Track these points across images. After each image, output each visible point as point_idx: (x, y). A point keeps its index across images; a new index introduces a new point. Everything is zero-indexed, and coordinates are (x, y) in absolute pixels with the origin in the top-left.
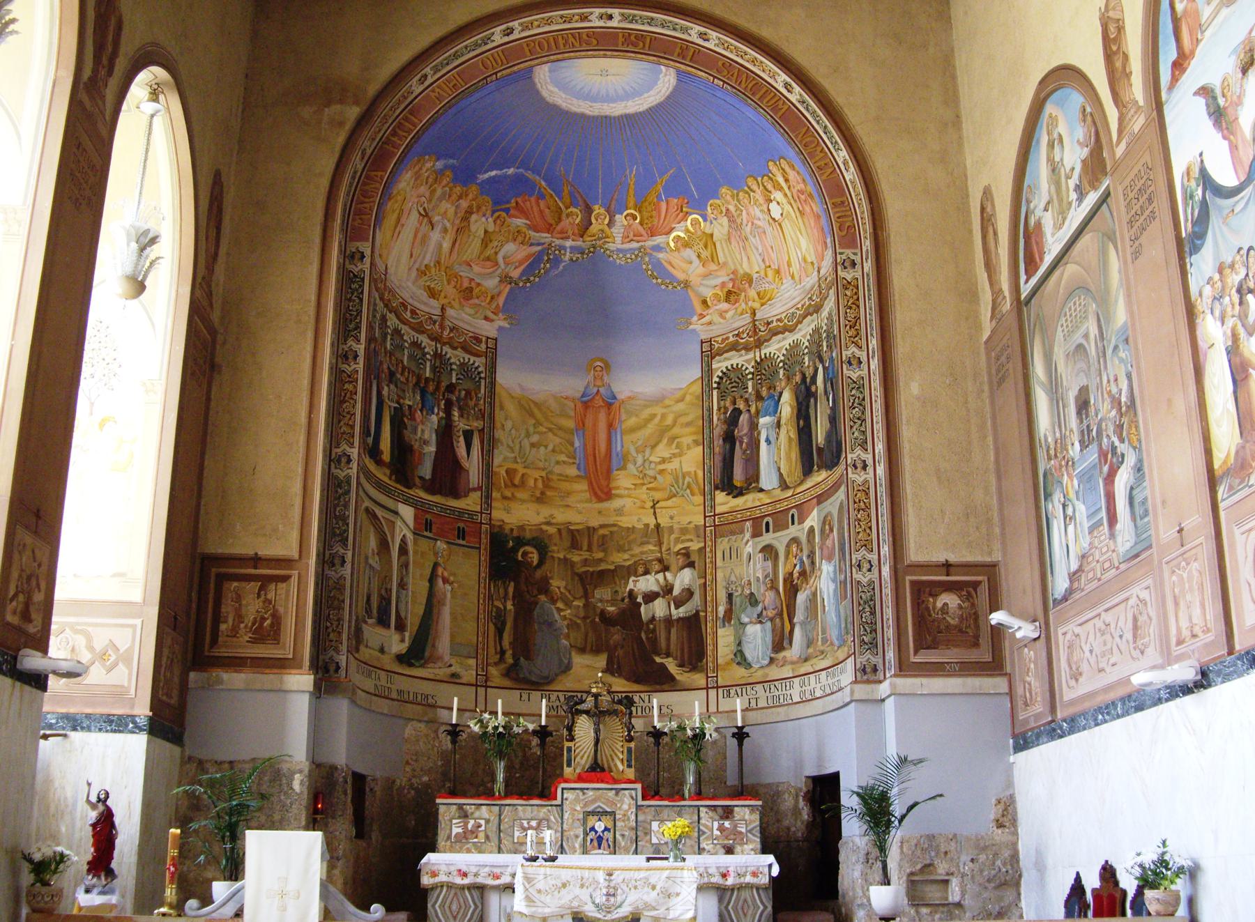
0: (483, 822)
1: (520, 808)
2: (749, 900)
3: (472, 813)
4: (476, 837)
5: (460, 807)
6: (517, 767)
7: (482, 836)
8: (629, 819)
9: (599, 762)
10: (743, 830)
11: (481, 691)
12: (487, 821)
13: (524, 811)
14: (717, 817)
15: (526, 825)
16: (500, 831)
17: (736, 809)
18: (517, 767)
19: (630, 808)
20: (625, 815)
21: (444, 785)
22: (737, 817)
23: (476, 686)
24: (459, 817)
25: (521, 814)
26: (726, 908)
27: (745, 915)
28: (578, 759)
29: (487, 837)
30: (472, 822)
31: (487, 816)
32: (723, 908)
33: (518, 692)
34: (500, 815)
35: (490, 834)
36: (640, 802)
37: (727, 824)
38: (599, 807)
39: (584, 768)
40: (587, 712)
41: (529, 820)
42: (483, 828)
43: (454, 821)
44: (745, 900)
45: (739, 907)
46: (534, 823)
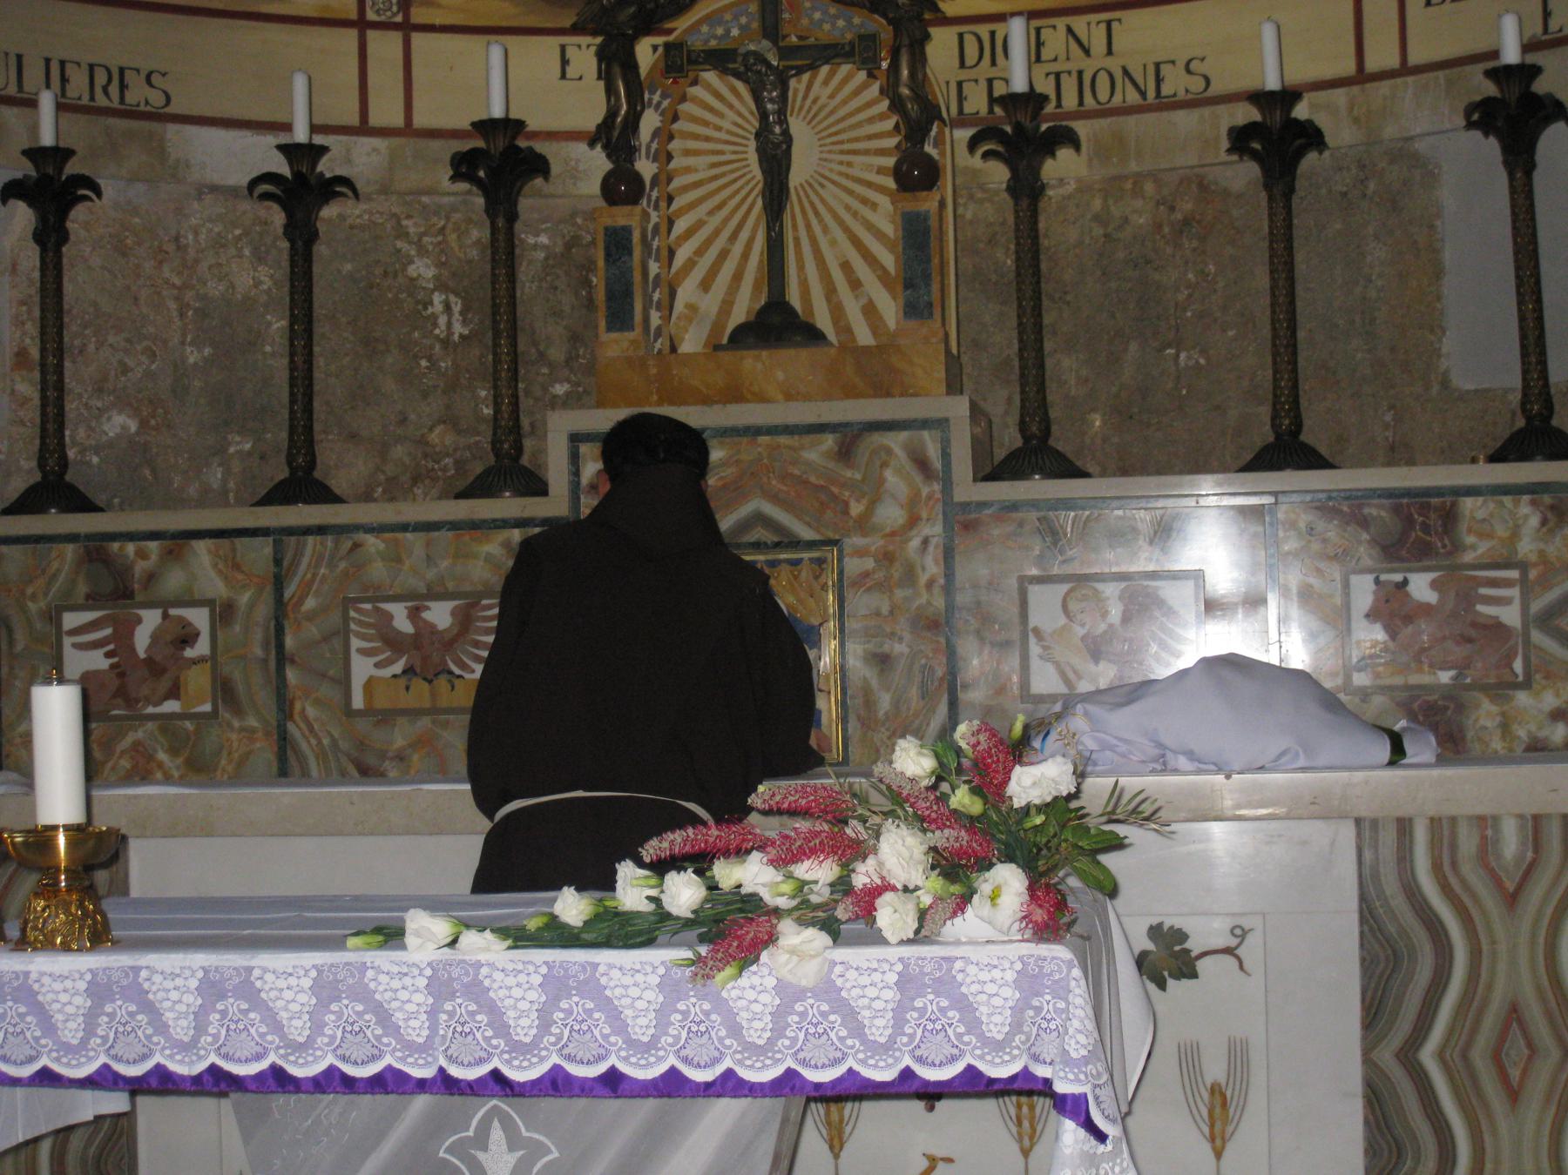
0: (199, 618)
1: (372, 543)
2: (1535, 1013)
3: (151, 578)
4: (174, 693)
5: (95, 549)
6: (557, 353)
7: (198, 681)
8: (910, 576)
9: (794, 299)
10: (1510, 616)
11: (386, 47)
12: (223, 613)
13: (395, 558)
14: (1366, 554)
15: (403, 624)
16: (282, 658)
17: (1468, 504)
18: (557, 353)
19: (913, 521)
20: (887, 558)
21: (221, 450)
22: (1476, 549)
23: (362, 25)
24: (92, 601)
25: (378, 571)
26: (1408, 1055)
27: (1514, 1095)
28: (687, 292)
29: (225, 691)
30: (150, 619)
31: (216, 587)
32: (1386, 1056)
33: (554, 42)
34: (279, 583)
35: (237, 676)
36: (967, 490)
37: (1421, 587)
38: (760, 519)
39: (717, 327)
40: (721, 59)
41: (417, 603)
42: (202, 647)
43: (71, 620)
44: (1514, 1013)
45: (1484, 1041)
46: (440, 615)
